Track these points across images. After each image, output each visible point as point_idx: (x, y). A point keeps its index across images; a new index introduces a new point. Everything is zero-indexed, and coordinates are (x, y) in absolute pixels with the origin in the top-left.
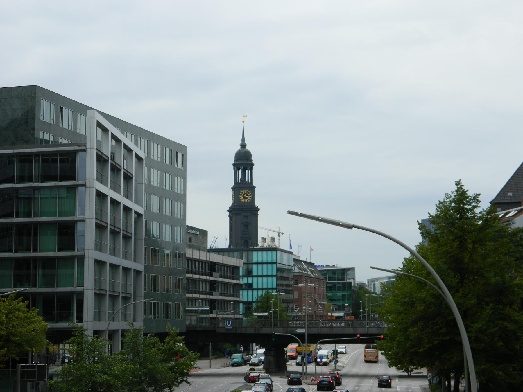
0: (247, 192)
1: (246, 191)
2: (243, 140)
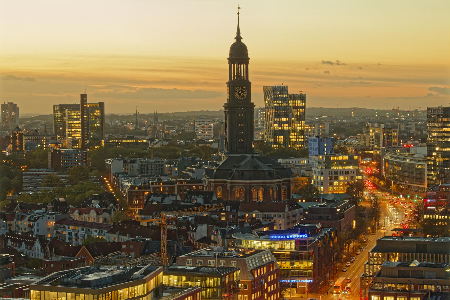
0: (242, 88)
1: (241, 87)
2: (239, 32)
